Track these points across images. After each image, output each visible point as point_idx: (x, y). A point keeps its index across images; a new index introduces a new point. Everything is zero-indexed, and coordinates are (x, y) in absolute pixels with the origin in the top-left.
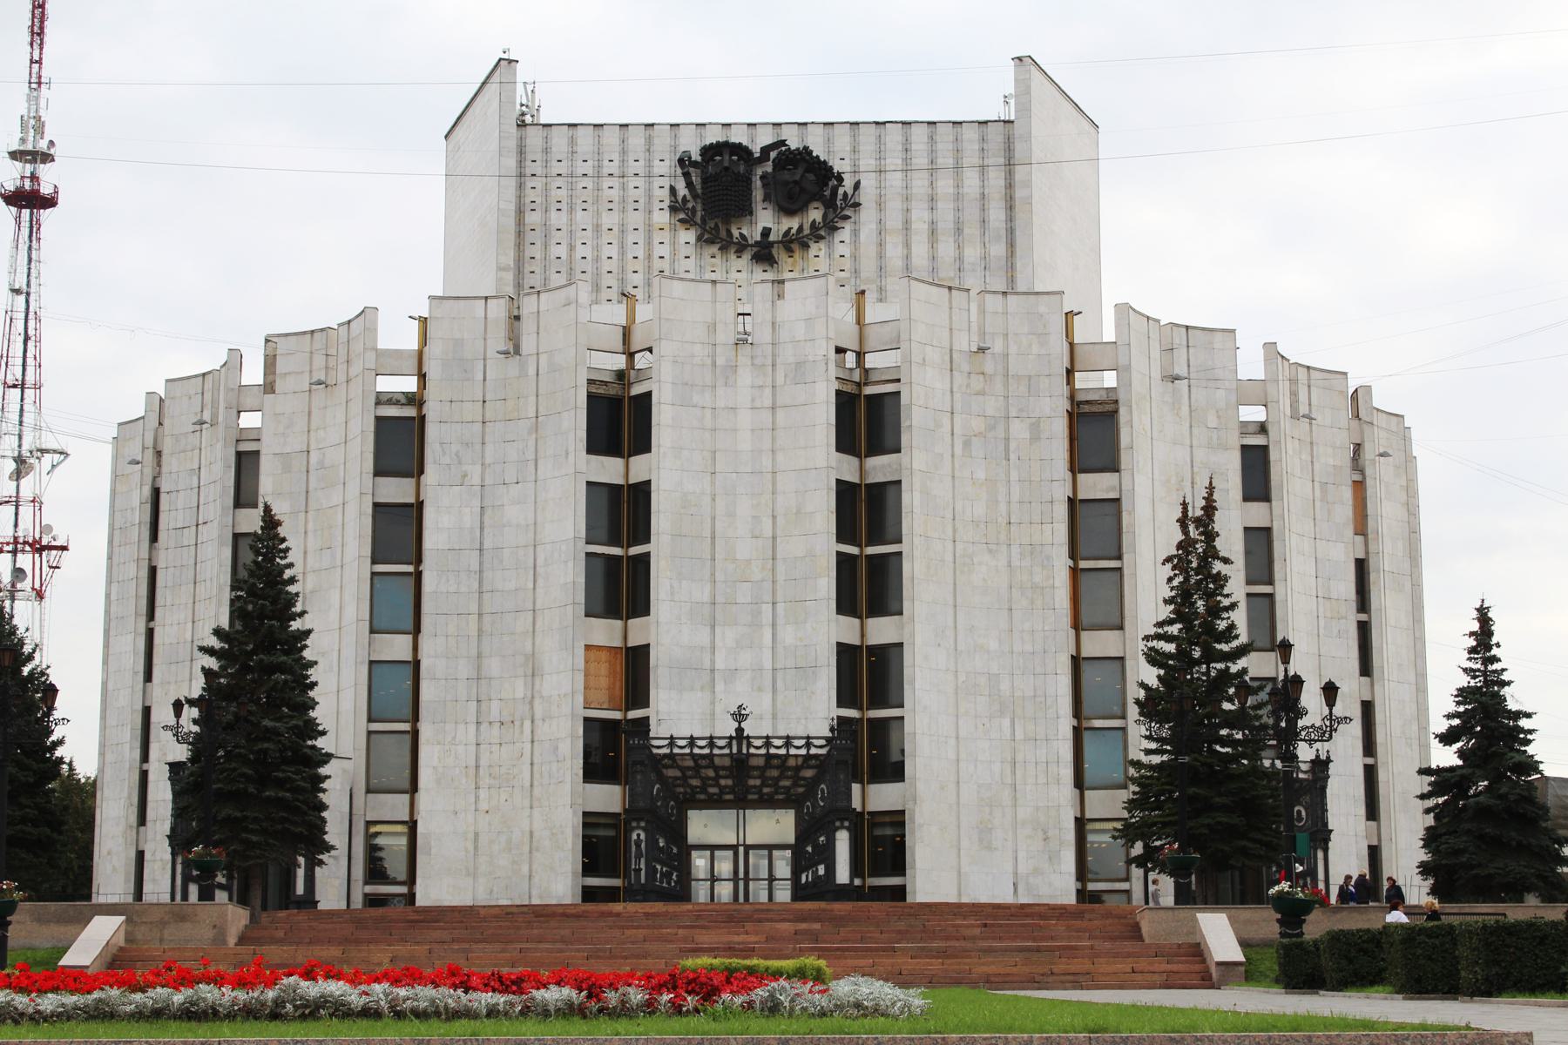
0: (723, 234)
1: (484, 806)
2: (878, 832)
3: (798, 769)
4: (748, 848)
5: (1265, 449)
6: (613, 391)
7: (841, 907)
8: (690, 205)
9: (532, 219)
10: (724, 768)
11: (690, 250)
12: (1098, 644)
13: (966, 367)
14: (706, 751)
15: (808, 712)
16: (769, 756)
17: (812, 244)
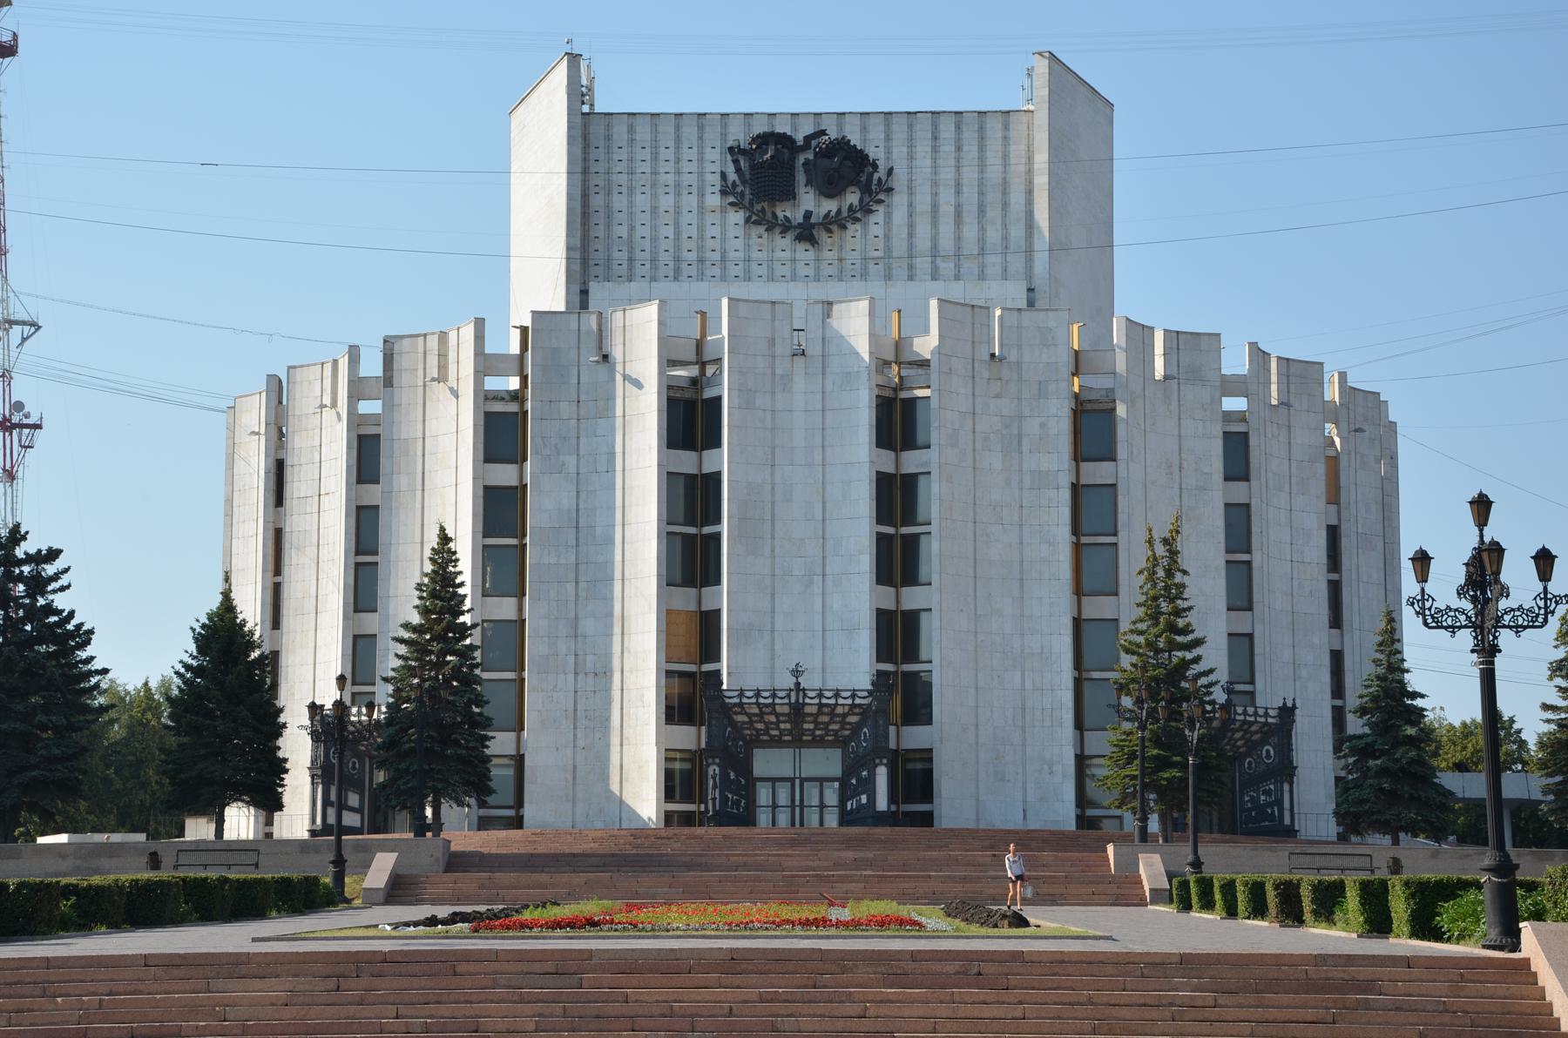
0: (769, 216)
1: (581, 743)
2: (910, 766)
3: (845, 715)
4: (803, 780)
5: (1246, 434)
6: (688, 395)
7: (882, 832)
8: (739, 189)
9: (597, 201)
11: (740, 232)
12: (1097, 608)
13: (986, 375)
15: (852, 667)
16: (821, 705)
17: (848, 225)
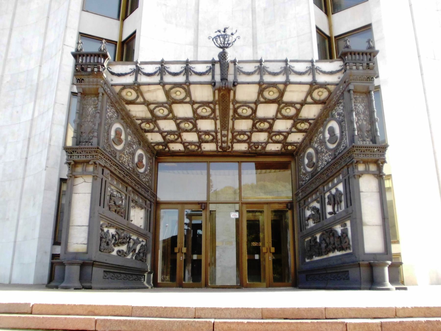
10: (204, 104)
14: (181, 79)
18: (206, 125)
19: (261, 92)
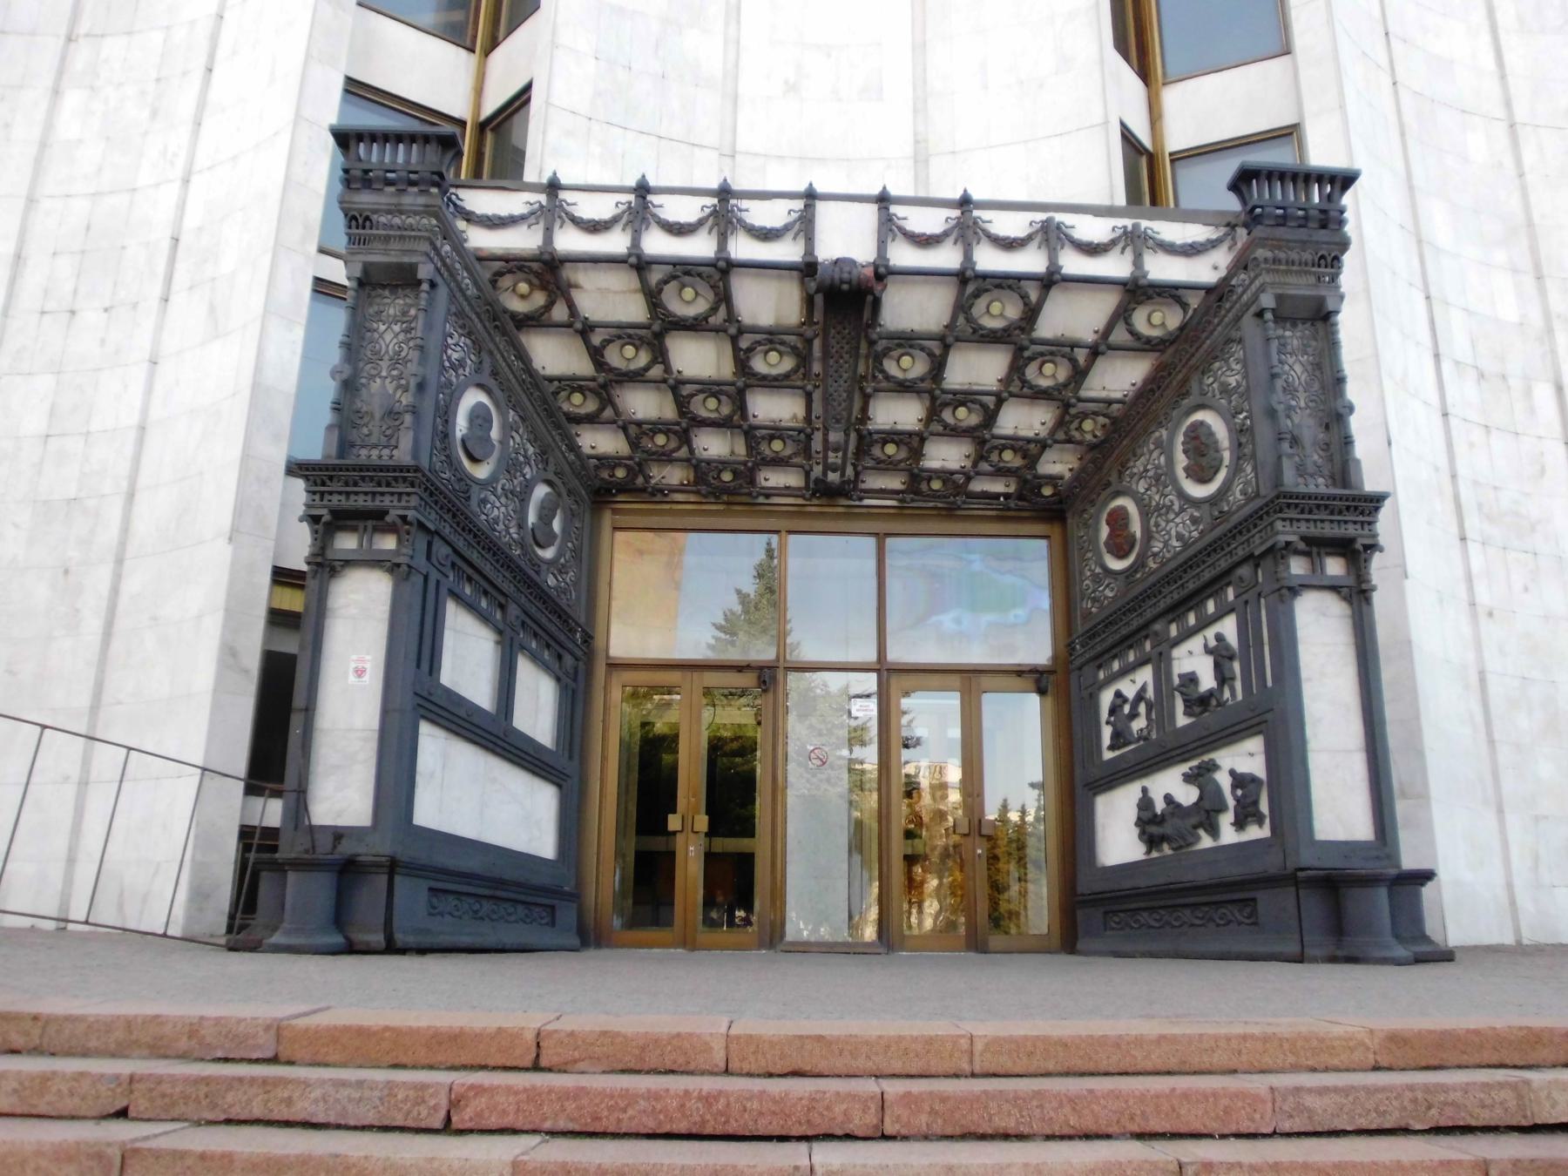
10: (772, 338)
14: (700, 247)
16: (968, 282)
18: (774, 408)
19: (962, 307)
